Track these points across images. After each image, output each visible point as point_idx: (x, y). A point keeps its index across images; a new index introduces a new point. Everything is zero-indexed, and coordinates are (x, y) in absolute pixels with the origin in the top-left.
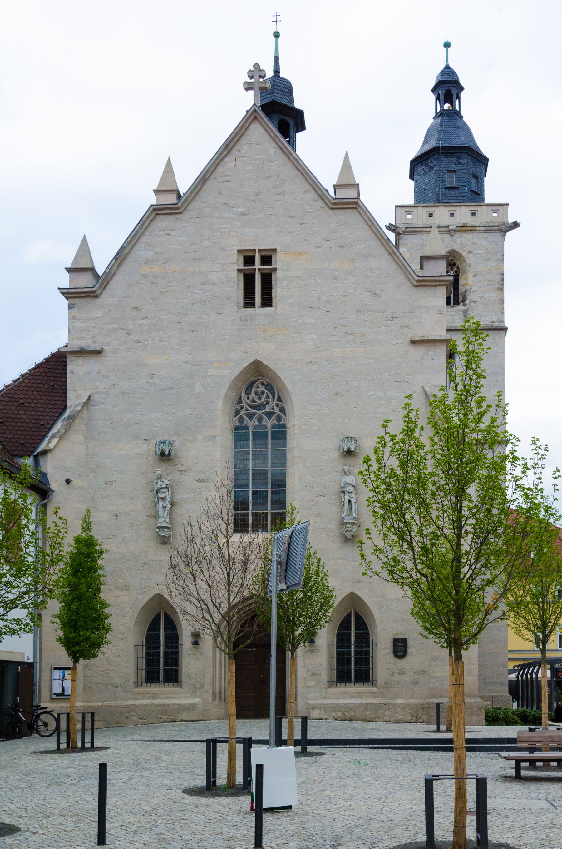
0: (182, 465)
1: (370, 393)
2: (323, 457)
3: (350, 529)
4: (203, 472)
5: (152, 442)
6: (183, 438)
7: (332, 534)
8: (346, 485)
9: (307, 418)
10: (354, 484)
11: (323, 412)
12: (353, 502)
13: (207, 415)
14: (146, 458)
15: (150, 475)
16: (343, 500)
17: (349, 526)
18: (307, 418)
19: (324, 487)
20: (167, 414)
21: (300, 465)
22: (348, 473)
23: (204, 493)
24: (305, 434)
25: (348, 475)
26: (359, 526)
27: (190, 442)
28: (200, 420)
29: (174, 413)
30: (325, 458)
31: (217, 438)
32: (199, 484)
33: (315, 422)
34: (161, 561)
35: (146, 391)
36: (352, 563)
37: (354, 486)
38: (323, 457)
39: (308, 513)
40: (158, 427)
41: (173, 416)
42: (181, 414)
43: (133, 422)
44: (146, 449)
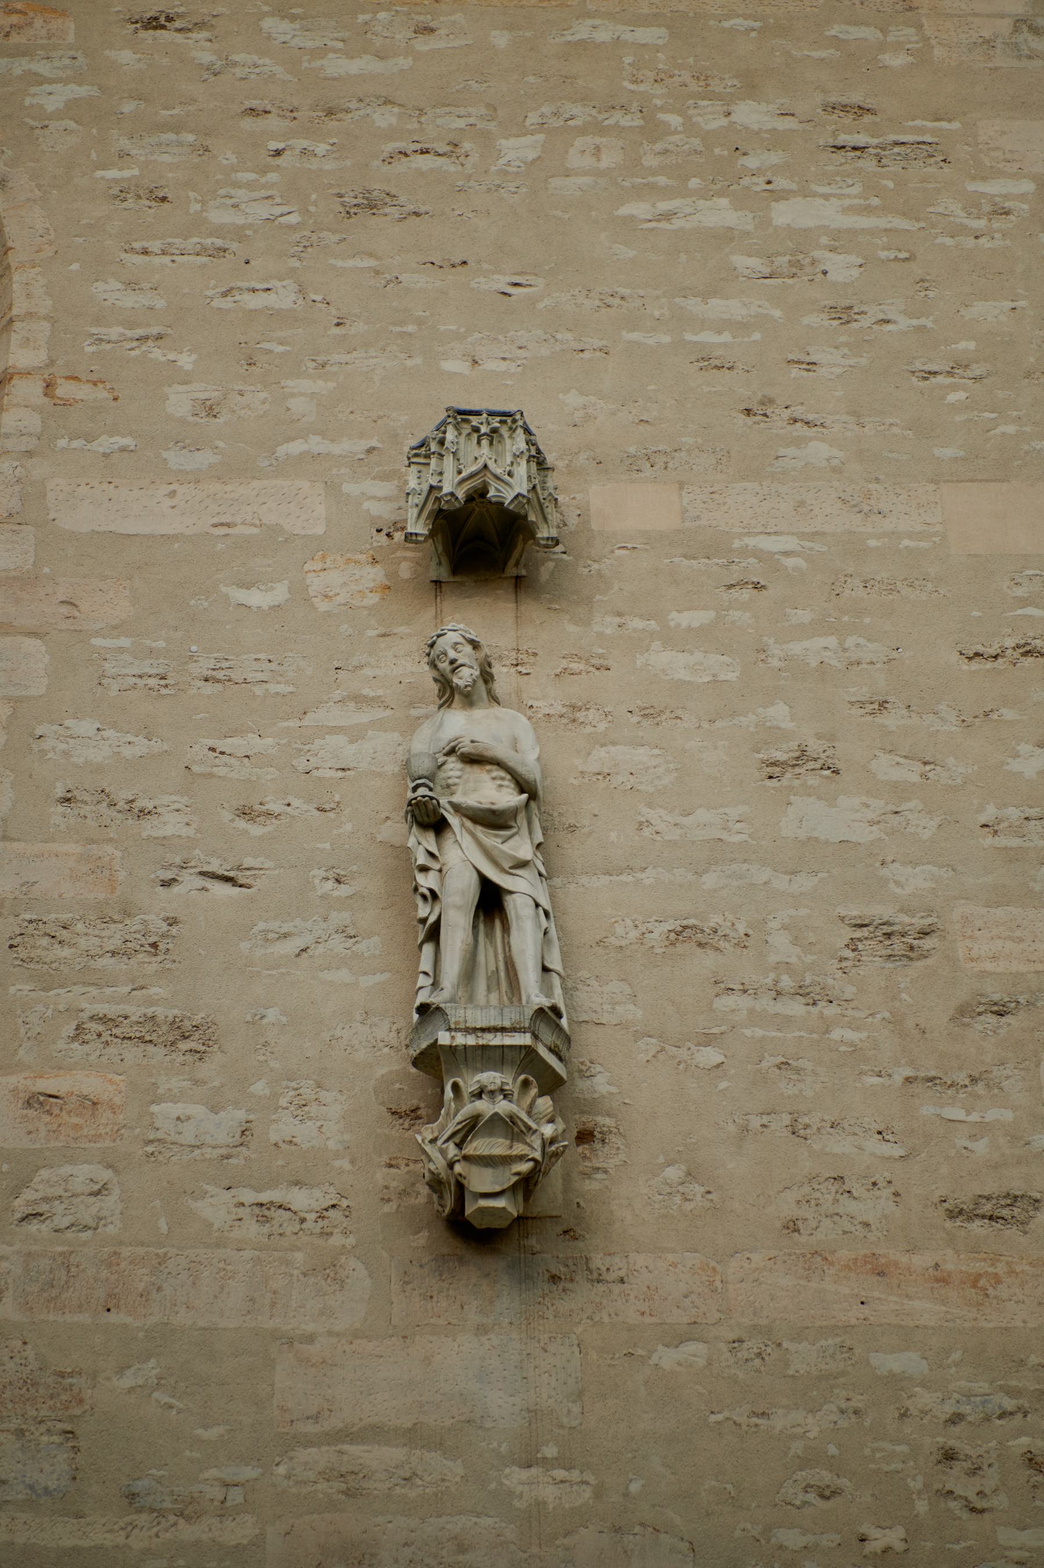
1: (638, 209)
2: (240, 595)
3: (503, 1107)
7: (300, 1199)
8: (453, 767)
9: (115, 332)
10: (528, 762)
11: (254, 302)
12: (518, 907)
16: (427, 882)
17: (491, 1078)
18: (115, 332)
19: (245, 813)
21: (32, 644)
22: (464, 677)
24: (90, 438)
25: (469, 699)
26: (585, 1137)
30: (256, 598)
33: (186, 361)
36: (516, 1477)
37: (523, 785)
38: (240, 595)
39: (73, 1011)
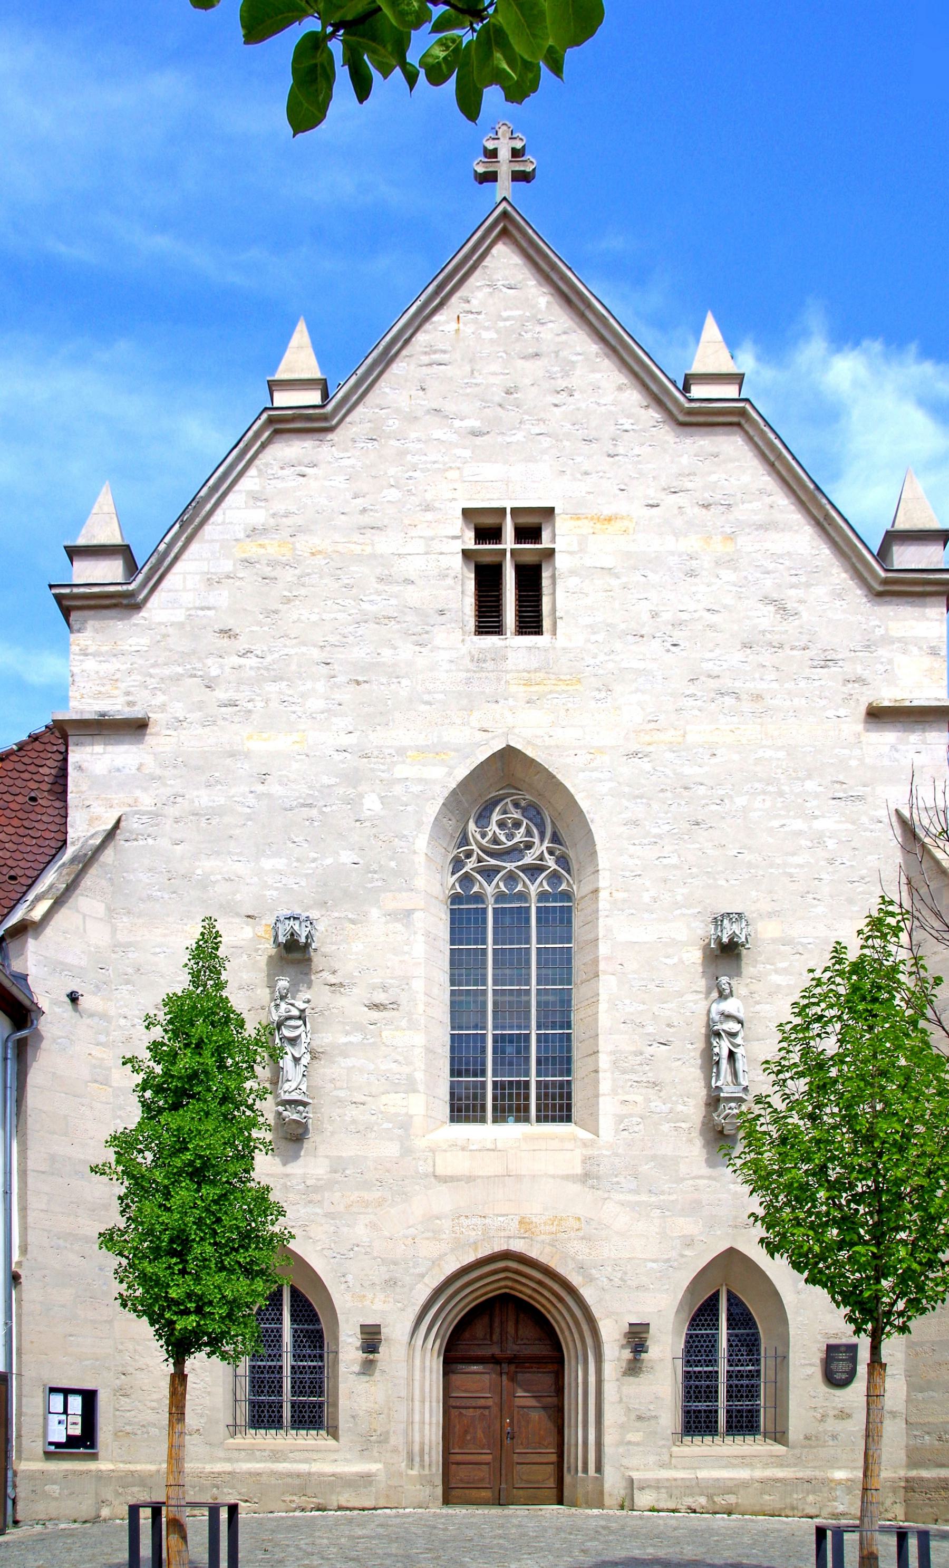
0: (334, 972)
4: (384, 988)
5: (264, 922)
6: (336, 914)
13: (393, 864)
14: (249, 955)
15: (259, 991)
20: (298, 860)
23: (384, 1034)
27: (353, 922)
28: (376, 876)
29: (314, 860)
31: (418, 915)
32: (375, 1015)
34: (287, 1175)
35: (249, 810)
40: (277, 889)
41: (313, 865)
42: (329, 861)
43: (219, 877)
44: (251, 935)
